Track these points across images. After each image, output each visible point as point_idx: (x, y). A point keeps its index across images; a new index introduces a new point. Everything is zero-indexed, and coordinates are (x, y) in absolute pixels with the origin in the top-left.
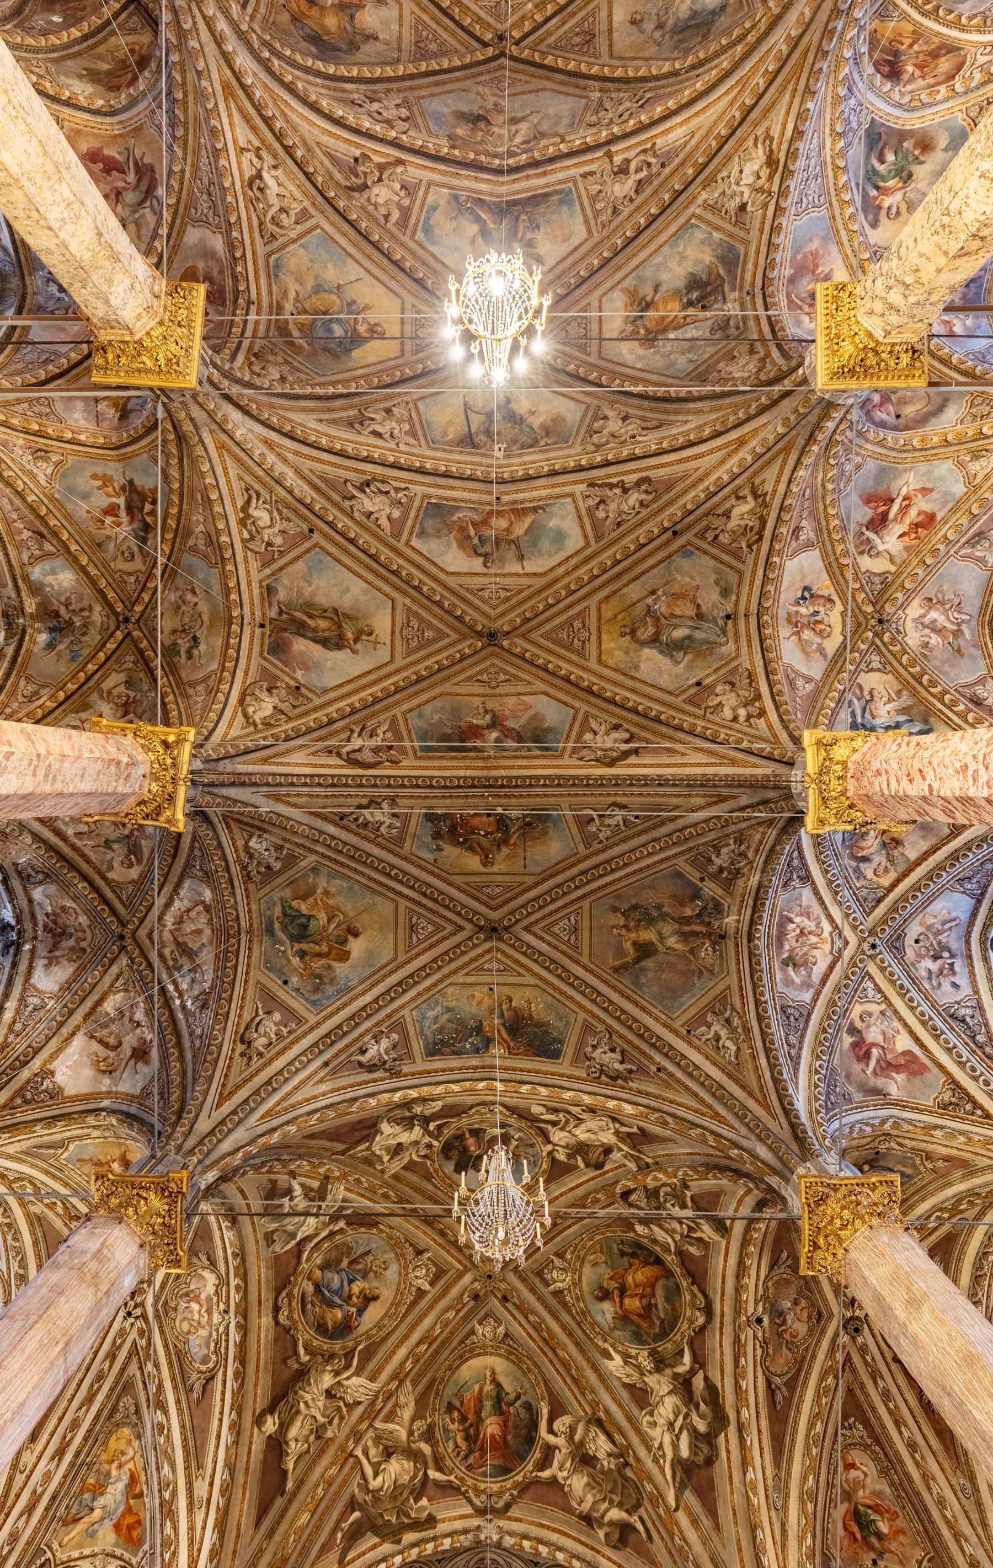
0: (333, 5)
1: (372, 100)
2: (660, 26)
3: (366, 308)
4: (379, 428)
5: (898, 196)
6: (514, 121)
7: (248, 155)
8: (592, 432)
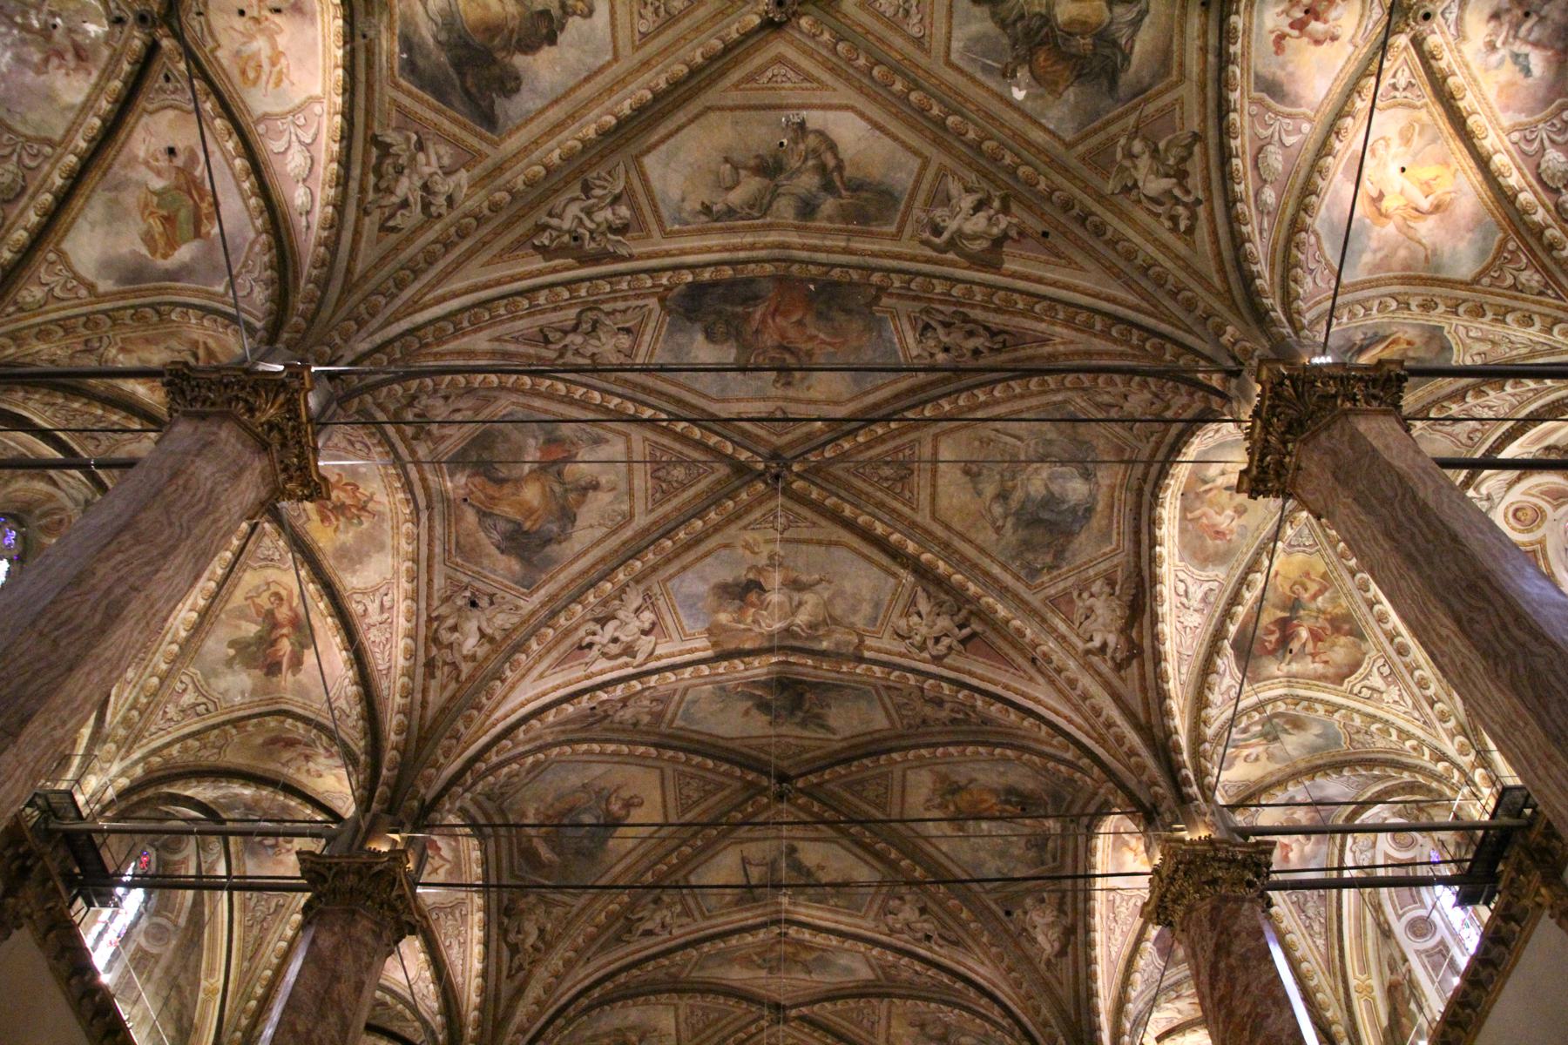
1: (603, 621)
2: (1003, 496)
3: (619, 788)
4: (649, 925)
5: (1261, 749)
6: (795, 585)
8: (886, 911)
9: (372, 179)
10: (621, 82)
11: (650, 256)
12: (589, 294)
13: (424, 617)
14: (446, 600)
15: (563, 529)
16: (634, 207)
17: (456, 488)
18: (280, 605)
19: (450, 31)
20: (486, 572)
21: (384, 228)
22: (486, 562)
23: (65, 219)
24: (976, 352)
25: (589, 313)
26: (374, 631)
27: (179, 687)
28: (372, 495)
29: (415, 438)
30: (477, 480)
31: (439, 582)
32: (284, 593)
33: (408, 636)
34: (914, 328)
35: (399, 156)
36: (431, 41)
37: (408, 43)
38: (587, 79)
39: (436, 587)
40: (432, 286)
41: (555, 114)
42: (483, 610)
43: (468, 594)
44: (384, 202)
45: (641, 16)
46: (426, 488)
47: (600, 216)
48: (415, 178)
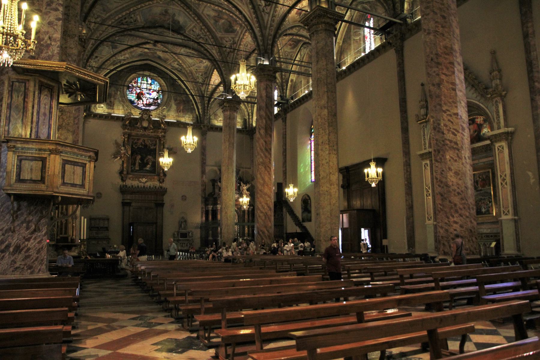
0: (223, 19)
7: (266, 11)
24: (125, 19)
29: (235, 43)
34: (138, 21)
46: (242, 32)
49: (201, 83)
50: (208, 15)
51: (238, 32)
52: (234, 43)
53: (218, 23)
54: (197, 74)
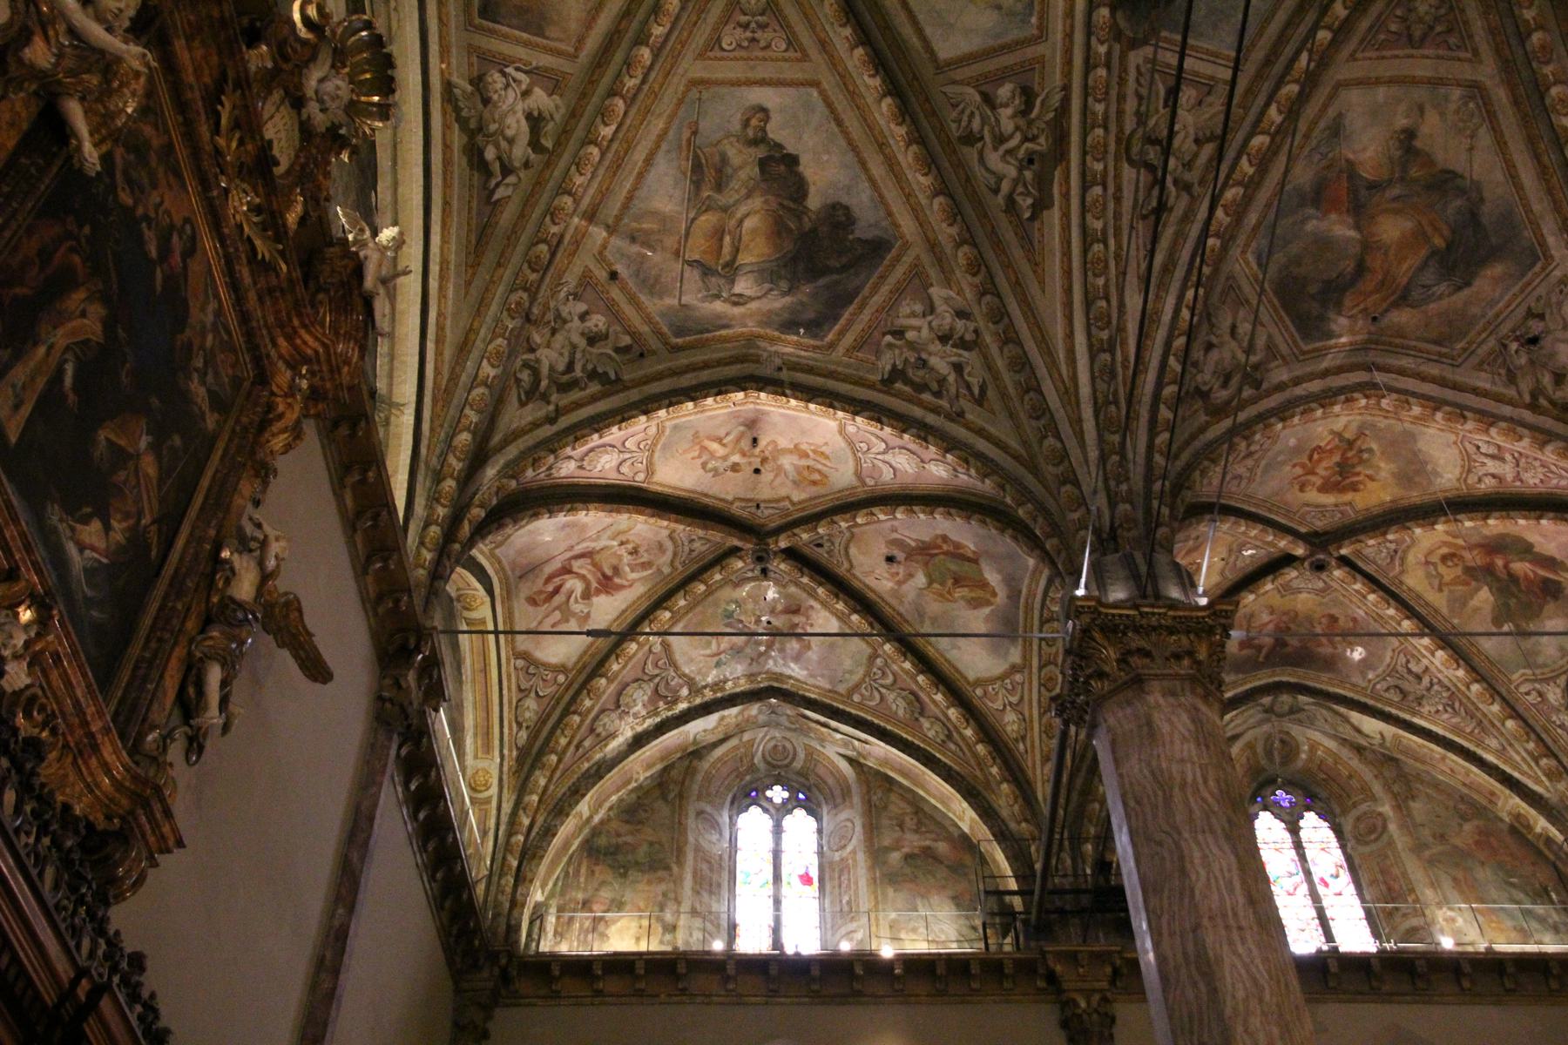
0: (1357, 227)
9: (926, 397)
10: (844, 79)
11: (1068, 62)
12: (1103, 159)
13: (1527, 415)
14: (1511, 378)
15: (1462, 192)
16: (1000, 78)
17: (1352, 332)
18: (1462, 558)
19: (780, 278)
20: (1491, 314)
21: (980, 400)
22: (1475, 310)
23: (945, 667)
25: (1135, 149)
26: (1526, 476)
27: (1533, 698)
28: (1332, 432)
29: (1257, 385)
30: (1347, 302)
31: (1483, 381)
32: (1445, 550)
33: (1542, 445)
35: (906, 360)
36: (788, 300)
37: (790, 326)
38: (839, 123)
39: (1488, 386)
40: (1052, 364)
41: (878, 169)
42: (1548, 331)
43: (1514, 346)
44: (953, 390)
45: (768, 47)
46: (1340, 370)
47: (1007, 126)
48: (932, 348)
49: (536, 373)
50: (1336, 131)
51: (1320, 353)
52: (1253, 377)
53: (1311, 211)
54: (577, 296)
